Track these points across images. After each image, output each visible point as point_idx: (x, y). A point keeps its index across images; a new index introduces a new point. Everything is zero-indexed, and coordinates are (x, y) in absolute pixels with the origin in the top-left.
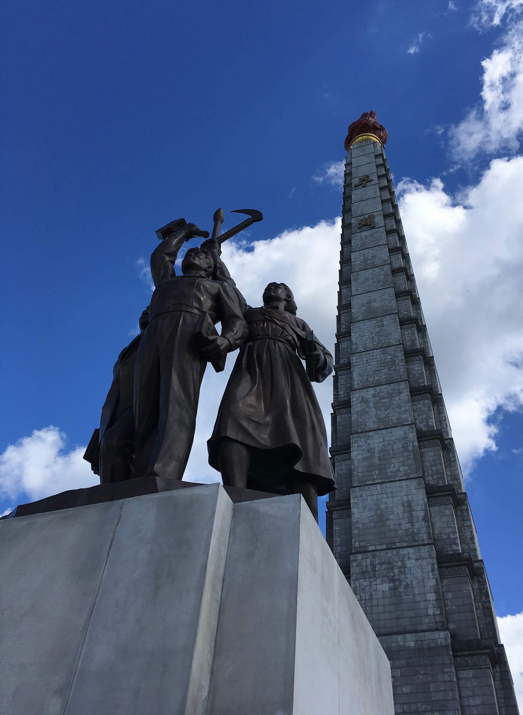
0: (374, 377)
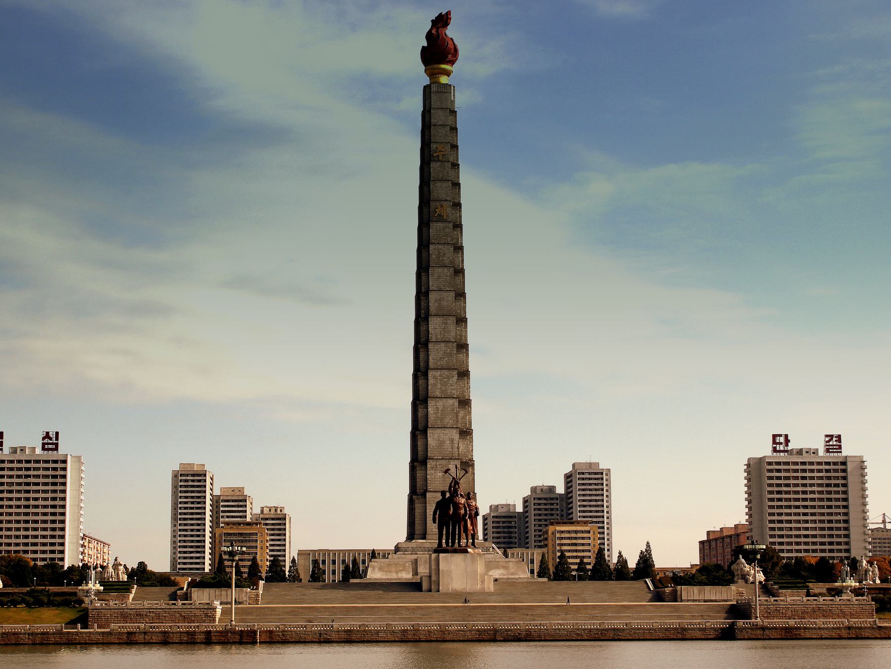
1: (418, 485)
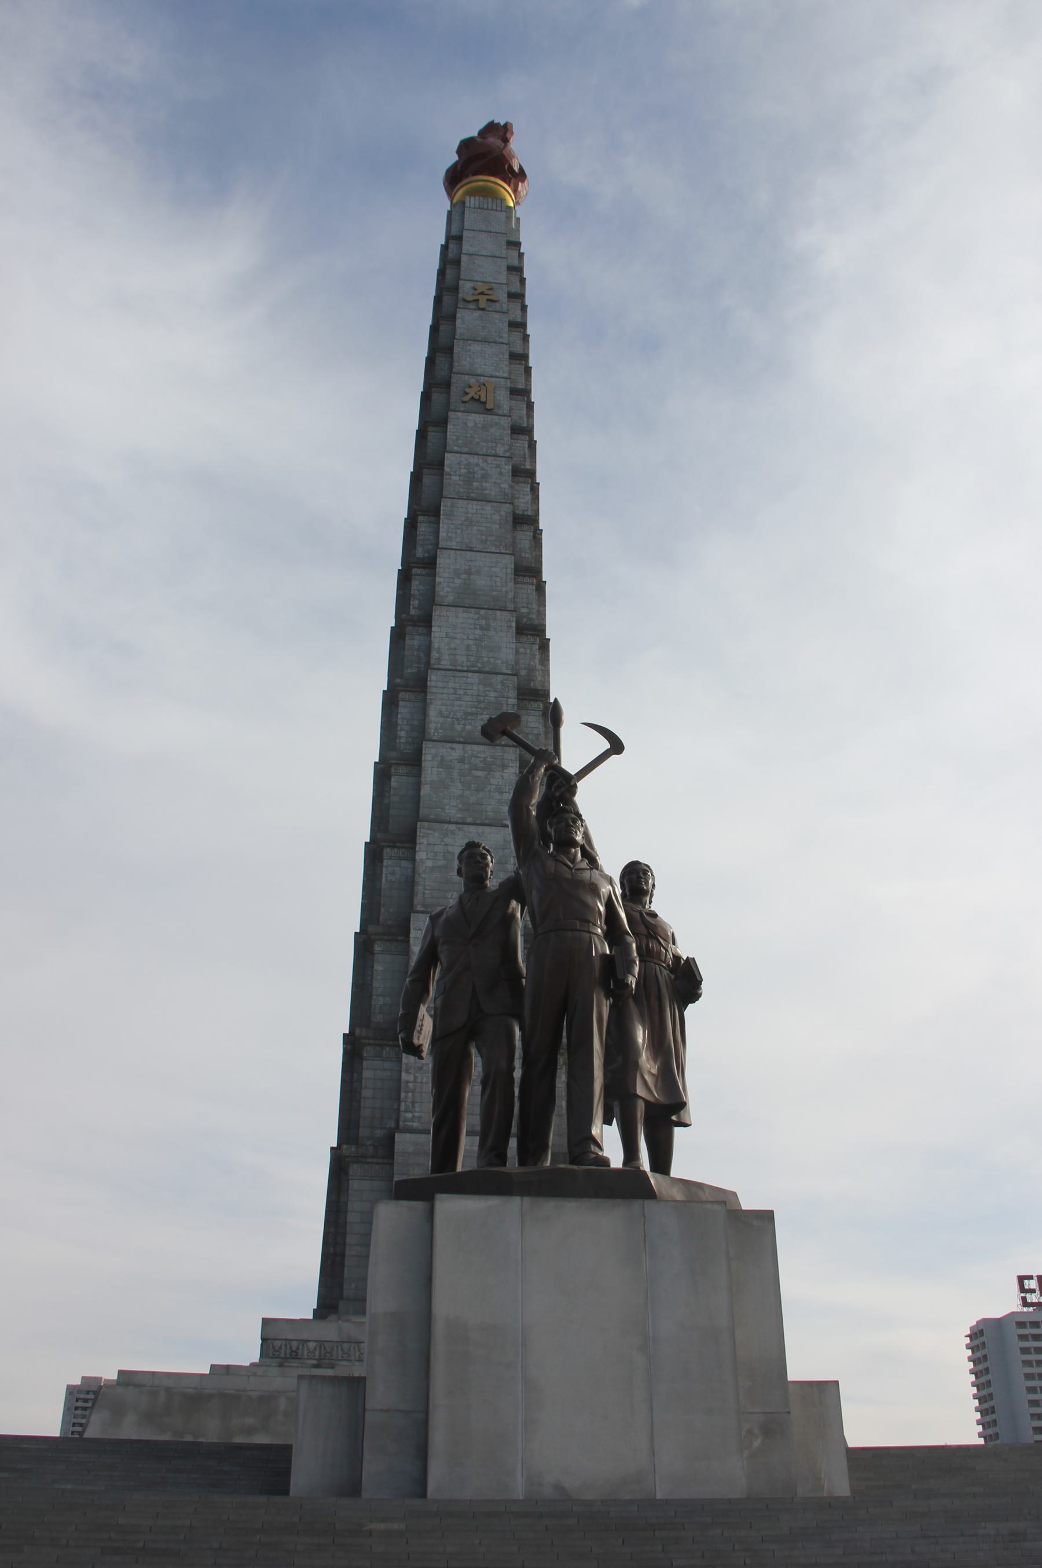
0: (465, 725)
1: (365, 1112)
